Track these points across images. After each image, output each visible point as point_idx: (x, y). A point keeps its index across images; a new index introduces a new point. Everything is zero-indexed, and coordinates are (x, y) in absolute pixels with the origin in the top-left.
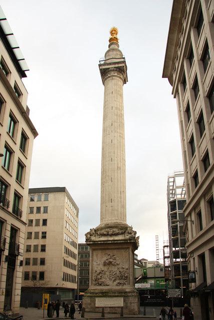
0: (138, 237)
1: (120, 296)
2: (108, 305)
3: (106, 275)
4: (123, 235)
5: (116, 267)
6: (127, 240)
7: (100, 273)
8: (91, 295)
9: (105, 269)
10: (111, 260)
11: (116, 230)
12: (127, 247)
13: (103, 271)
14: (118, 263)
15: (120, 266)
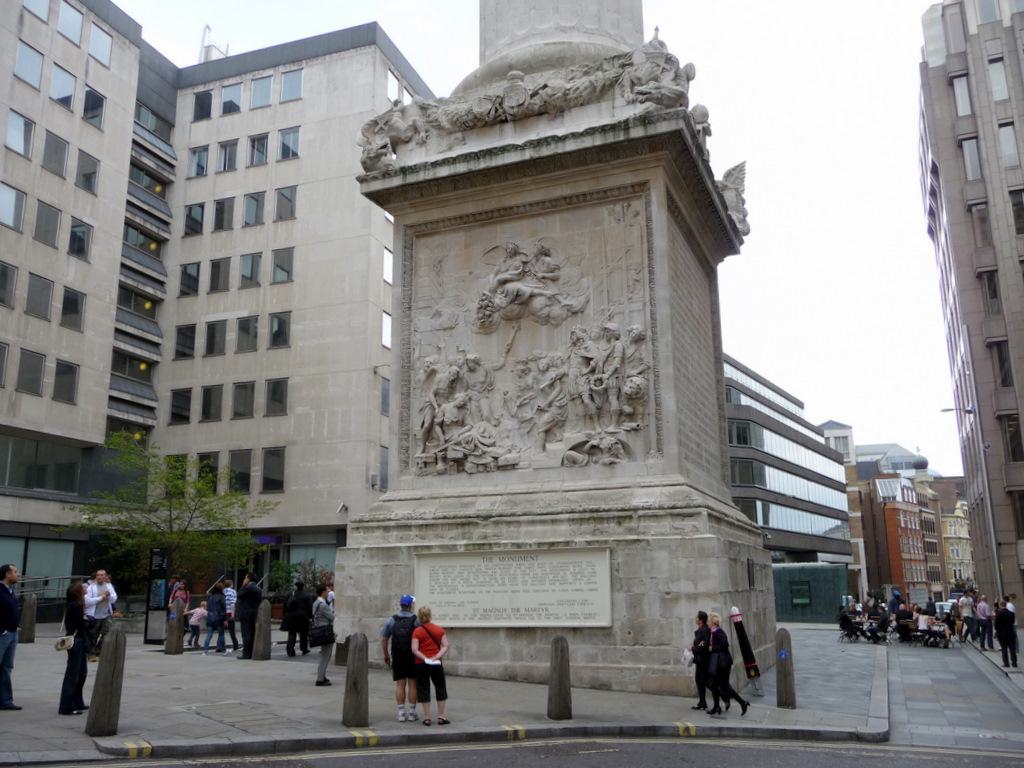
0: (737, 173)
1: (591, 548)
2: (498, 612)
3: (497, 397)
4: (604, 105)
5: (563, 335)
6: (625, 125)
7: (454, 383)
8: (393, 540)
9: (488, 350)
10: (526, 287)
11: (557, 81)
12: (629, 179)
13: (473, 366)
14: (576, 302)
15: (591, 324)
